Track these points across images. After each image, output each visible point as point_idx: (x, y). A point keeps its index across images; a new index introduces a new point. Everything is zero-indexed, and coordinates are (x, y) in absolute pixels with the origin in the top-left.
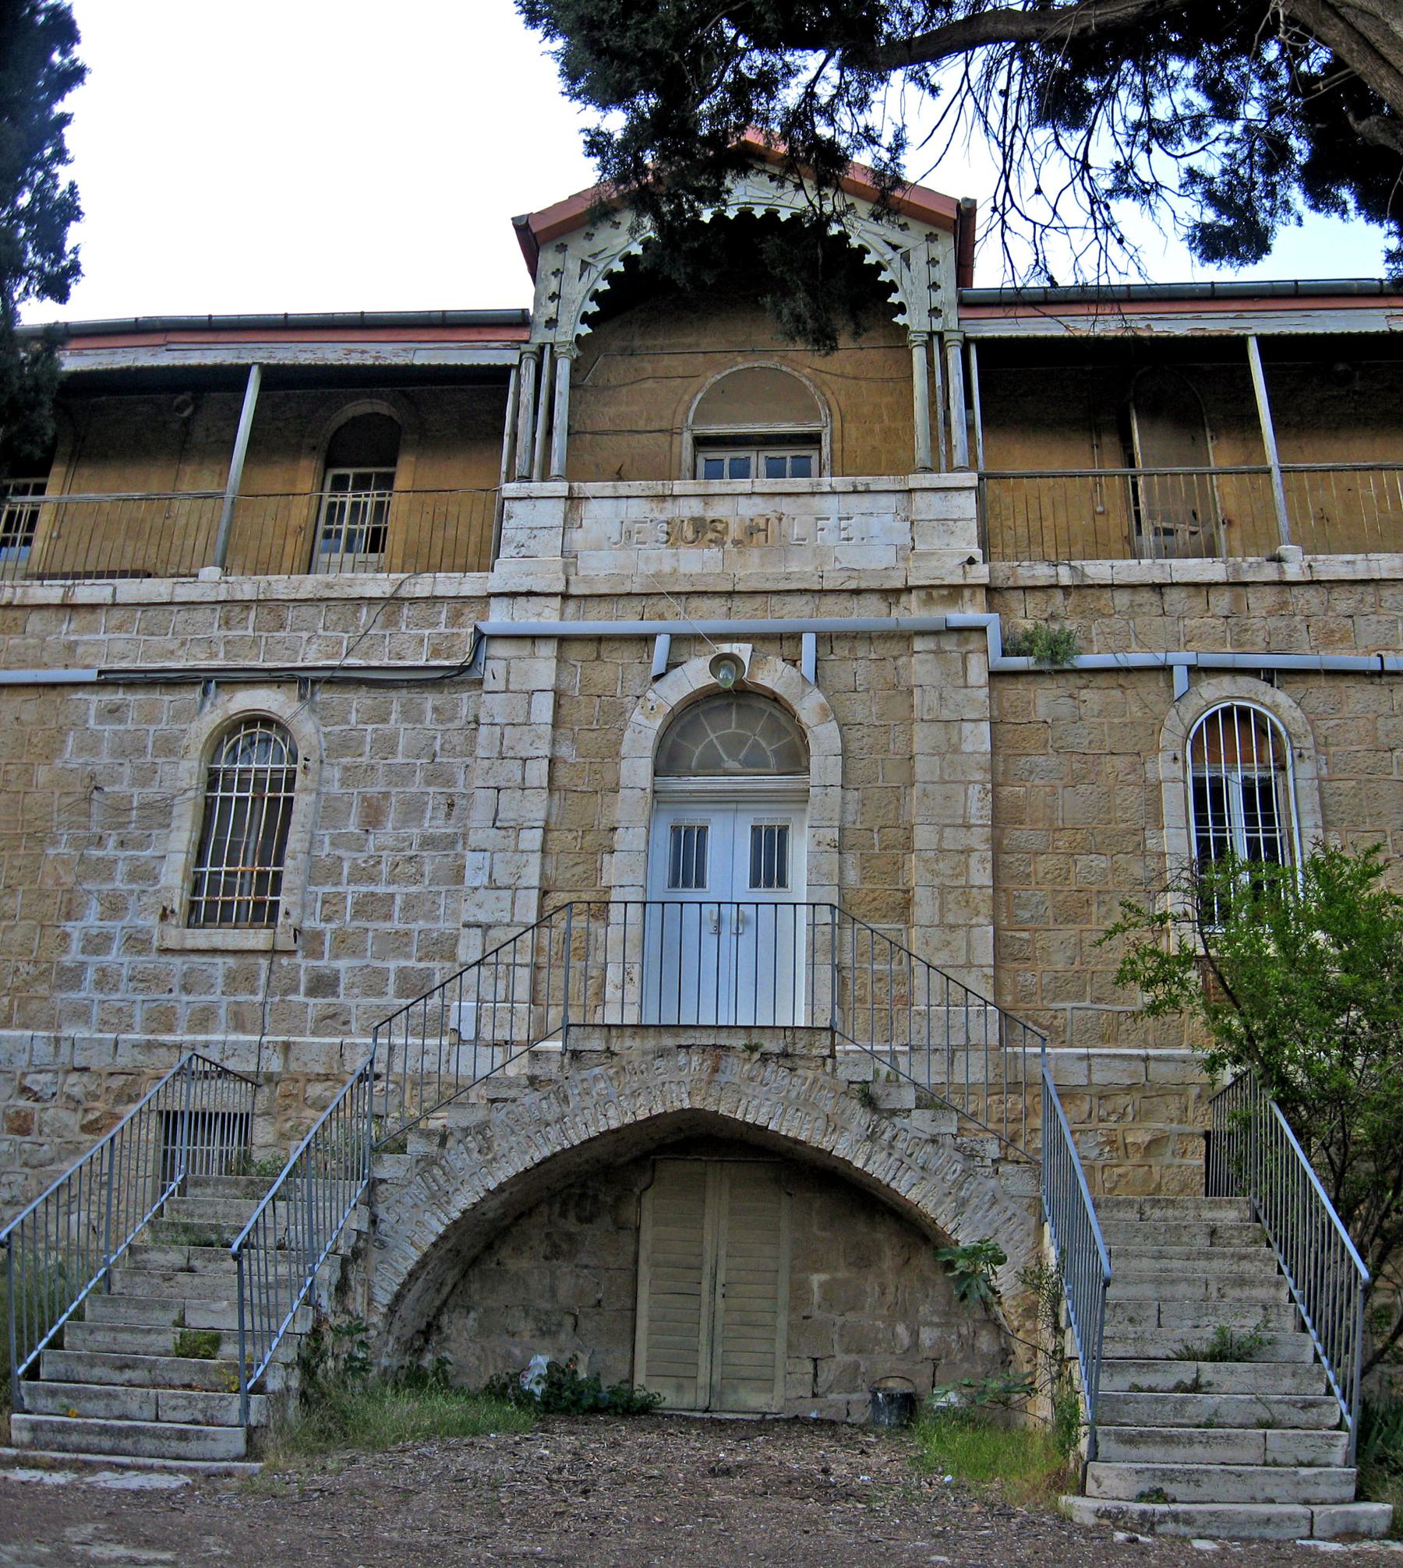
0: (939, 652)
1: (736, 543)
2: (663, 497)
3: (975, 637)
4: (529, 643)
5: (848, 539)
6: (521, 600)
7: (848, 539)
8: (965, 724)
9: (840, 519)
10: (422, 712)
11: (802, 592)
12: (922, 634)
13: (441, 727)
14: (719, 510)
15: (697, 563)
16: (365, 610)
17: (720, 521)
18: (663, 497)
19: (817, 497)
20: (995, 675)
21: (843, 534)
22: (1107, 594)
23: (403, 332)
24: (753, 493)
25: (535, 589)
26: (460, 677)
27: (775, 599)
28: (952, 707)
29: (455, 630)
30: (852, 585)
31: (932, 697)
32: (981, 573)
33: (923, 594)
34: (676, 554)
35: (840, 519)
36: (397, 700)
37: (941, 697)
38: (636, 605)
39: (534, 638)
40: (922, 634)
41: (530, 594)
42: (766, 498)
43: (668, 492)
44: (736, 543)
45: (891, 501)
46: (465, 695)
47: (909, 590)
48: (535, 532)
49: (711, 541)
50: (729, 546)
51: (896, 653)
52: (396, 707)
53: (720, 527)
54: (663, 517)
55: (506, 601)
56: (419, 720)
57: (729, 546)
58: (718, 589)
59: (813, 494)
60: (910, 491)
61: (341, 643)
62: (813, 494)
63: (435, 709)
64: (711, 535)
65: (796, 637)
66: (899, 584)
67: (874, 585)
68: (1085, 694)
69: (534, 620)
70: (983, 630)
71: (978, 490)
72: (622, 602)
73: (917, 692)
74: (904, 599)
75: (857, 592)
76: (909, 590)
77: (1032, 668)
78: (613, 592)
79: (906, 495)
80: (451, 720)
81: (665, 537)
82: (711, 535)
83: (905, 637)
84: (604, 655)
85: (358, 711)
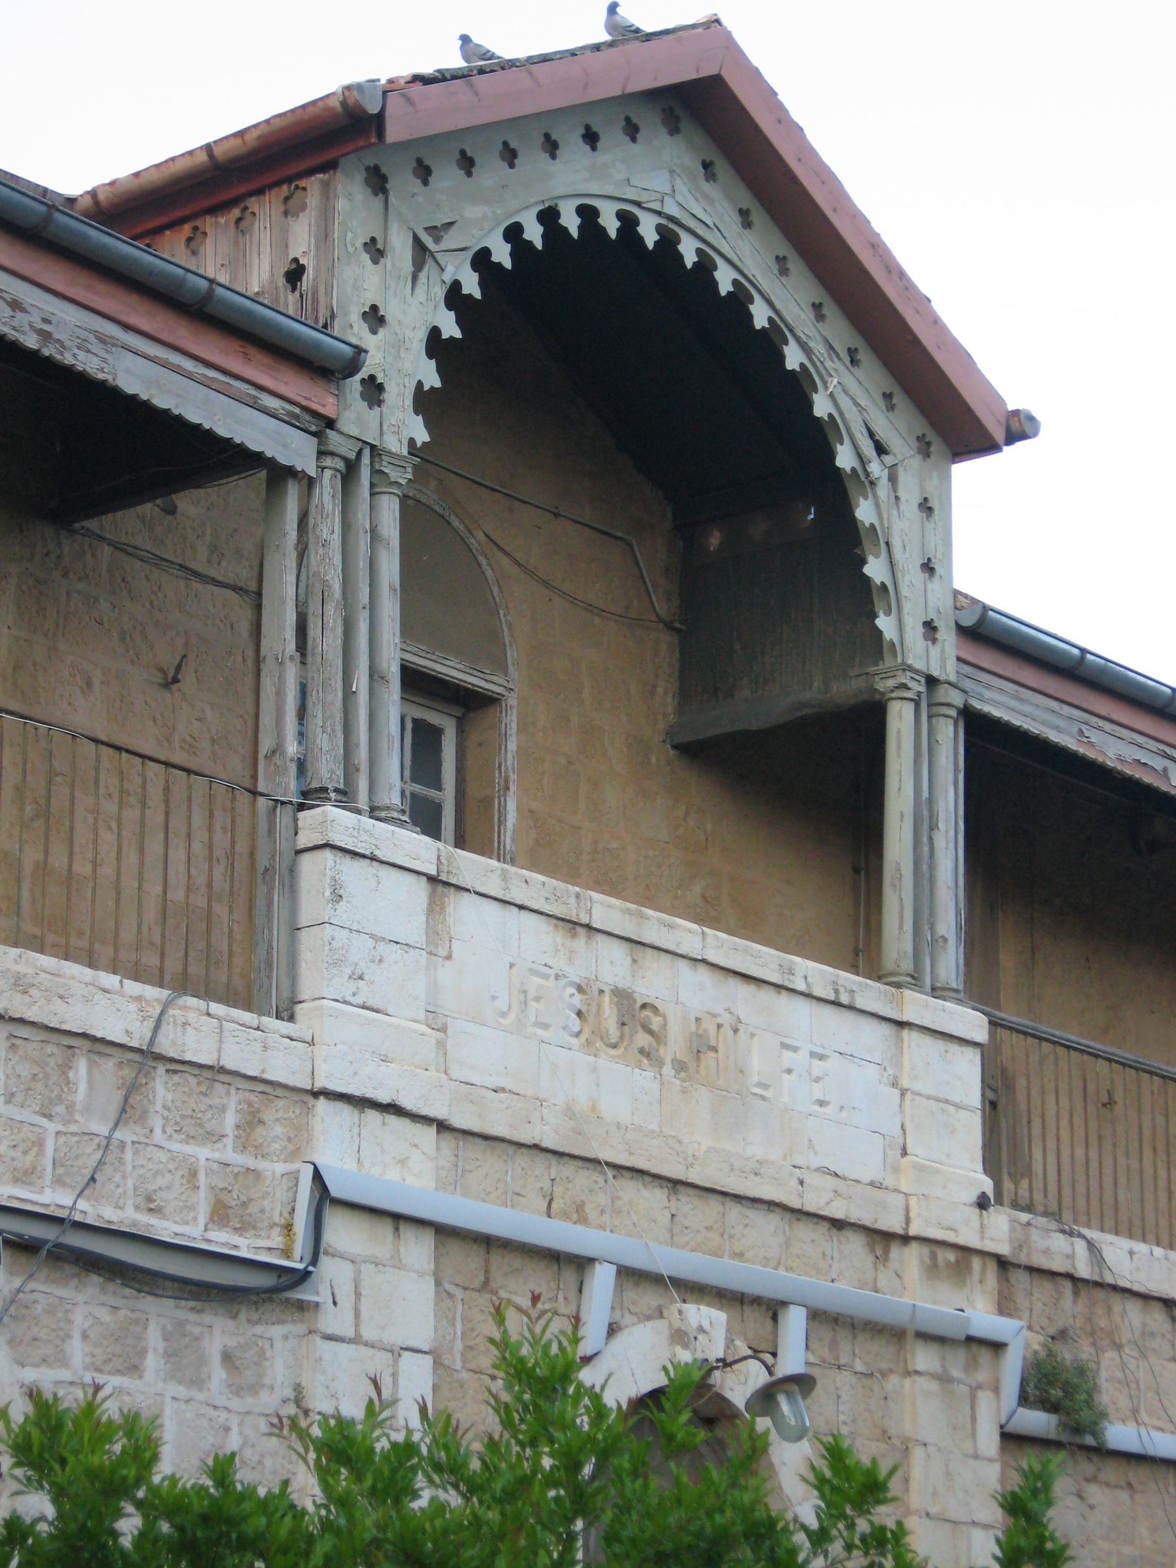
0: (944, 1378)
1: (680, 1066)
2: (572, 925)
3: (985, 1355)
4: (387, 1227)
6: (372, 1116)
10: (202, 1361)
11: (772, 1205)
12: (924, 1336)
13: (235, 1404)
14: (655, 982)
15: (619, 1101)
16: (82, 1066)
17: (655, 1009)
19: (784, 997)
20: (1011, 1439)
22: (1116, 1299)
23: (102, 287)
24: (704, 961)
25: (407, 1103)
26: (279, 1289)
27: (735, 1211)
29: (251, 1163)
32: (998, 1231)
33: (925, 1250)
36: (158, 1317)
38: (540, 1171)
39: (398, 1218)
40: (924, 1336)
41: (393, 1109)
42: (719, 976)
43: (584, 919)
45: (873, 1036)
46: (277, 1331)
47: (906, 1239)
48: (383, 948)
49: (642, 1051)
51: (884, 1366)
52: (154, 1338)
53: (656, 1023)
54: (575, 973)
55: (345, 1112)
56: (198, 1382)
57: (668, 1070)
59: (779, 987)
60: (901, 1024)
61: (40, 1144)
62: (779, 987)
63: (227, 1357)
65: (773, 1309)
66: (896, 1226)
68: (1094, 1492)
69: (394, 1175)
70: (997, 1347)
71: (989, 1054)
72: (523, 1159)
74: (895, 1251)
75: (838, 1224)
76: (906, 1239)
77: (1052, 1435)
79: (886, 1029)
80: (255, 1388)
81: (576, 1024)
83: (893, 1334)
84: (497, 1281)
85: (85, 1336)
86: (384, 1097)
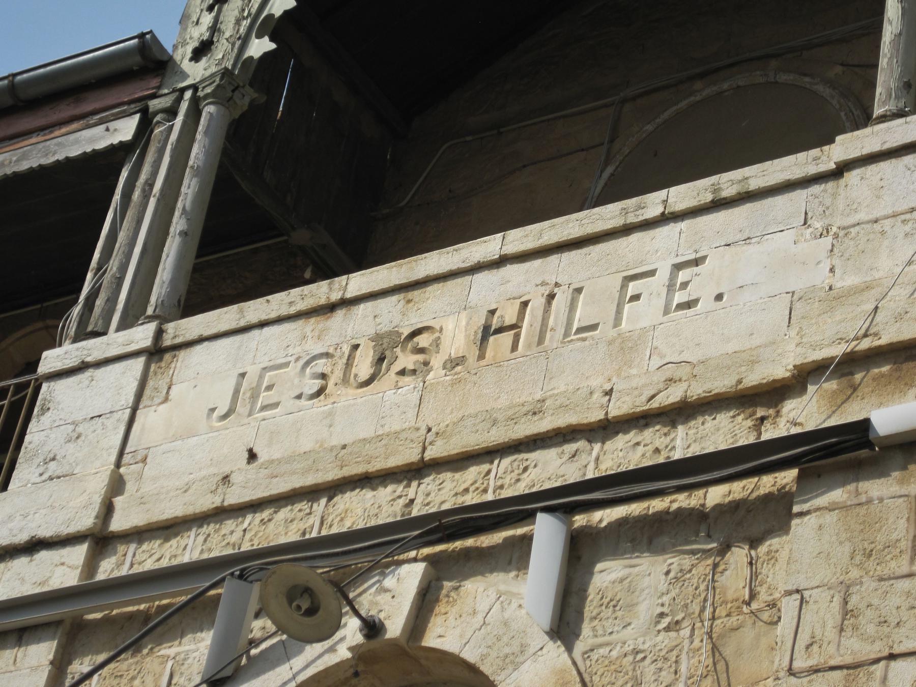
5: (688, 305)
7: (688, 305)
8: (895, 665)
9: (678, 267)
18: (331, 308)
21: (679, 297)
25: (46, 532)
28: (871, 629)
30: (673, 396)
31: (823, 612)
34: (331, 414)
35: (678, 267)
37: (846, 612)
44: (454, 363)
49: (402, 373)
50: (437, 374)
58: (393, 462)
64: (406, 360)
66: (780, 370)
67: (722, 384)
73: (789, 606)
78: (190, 510)
82: (406, 360)
86: (22, 537)
